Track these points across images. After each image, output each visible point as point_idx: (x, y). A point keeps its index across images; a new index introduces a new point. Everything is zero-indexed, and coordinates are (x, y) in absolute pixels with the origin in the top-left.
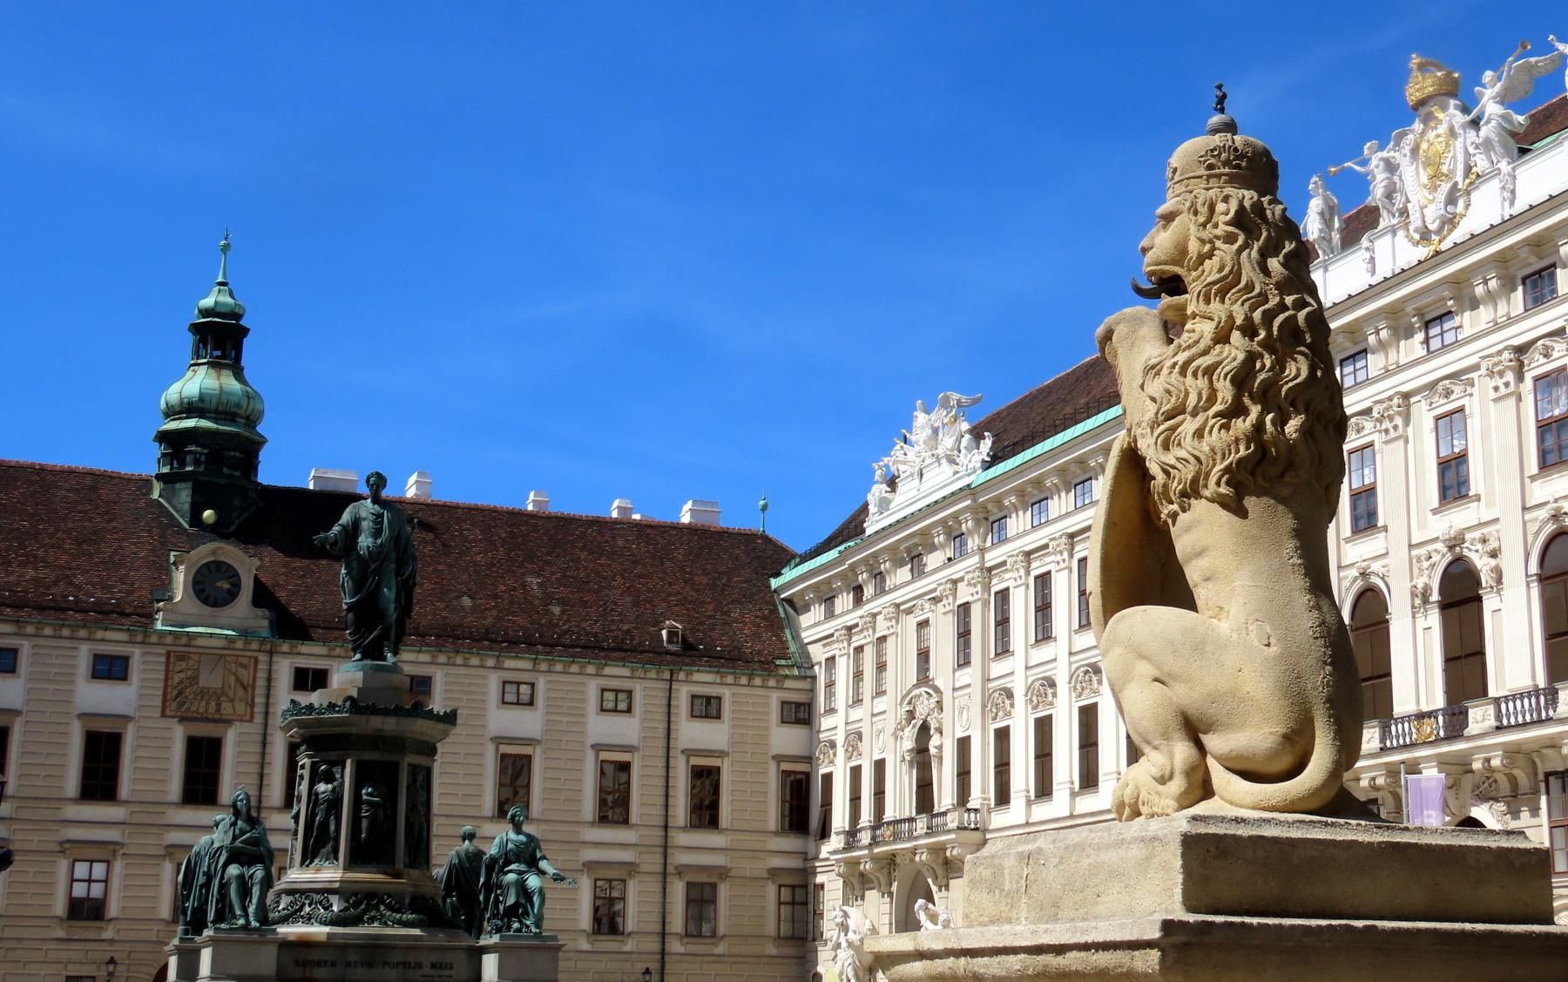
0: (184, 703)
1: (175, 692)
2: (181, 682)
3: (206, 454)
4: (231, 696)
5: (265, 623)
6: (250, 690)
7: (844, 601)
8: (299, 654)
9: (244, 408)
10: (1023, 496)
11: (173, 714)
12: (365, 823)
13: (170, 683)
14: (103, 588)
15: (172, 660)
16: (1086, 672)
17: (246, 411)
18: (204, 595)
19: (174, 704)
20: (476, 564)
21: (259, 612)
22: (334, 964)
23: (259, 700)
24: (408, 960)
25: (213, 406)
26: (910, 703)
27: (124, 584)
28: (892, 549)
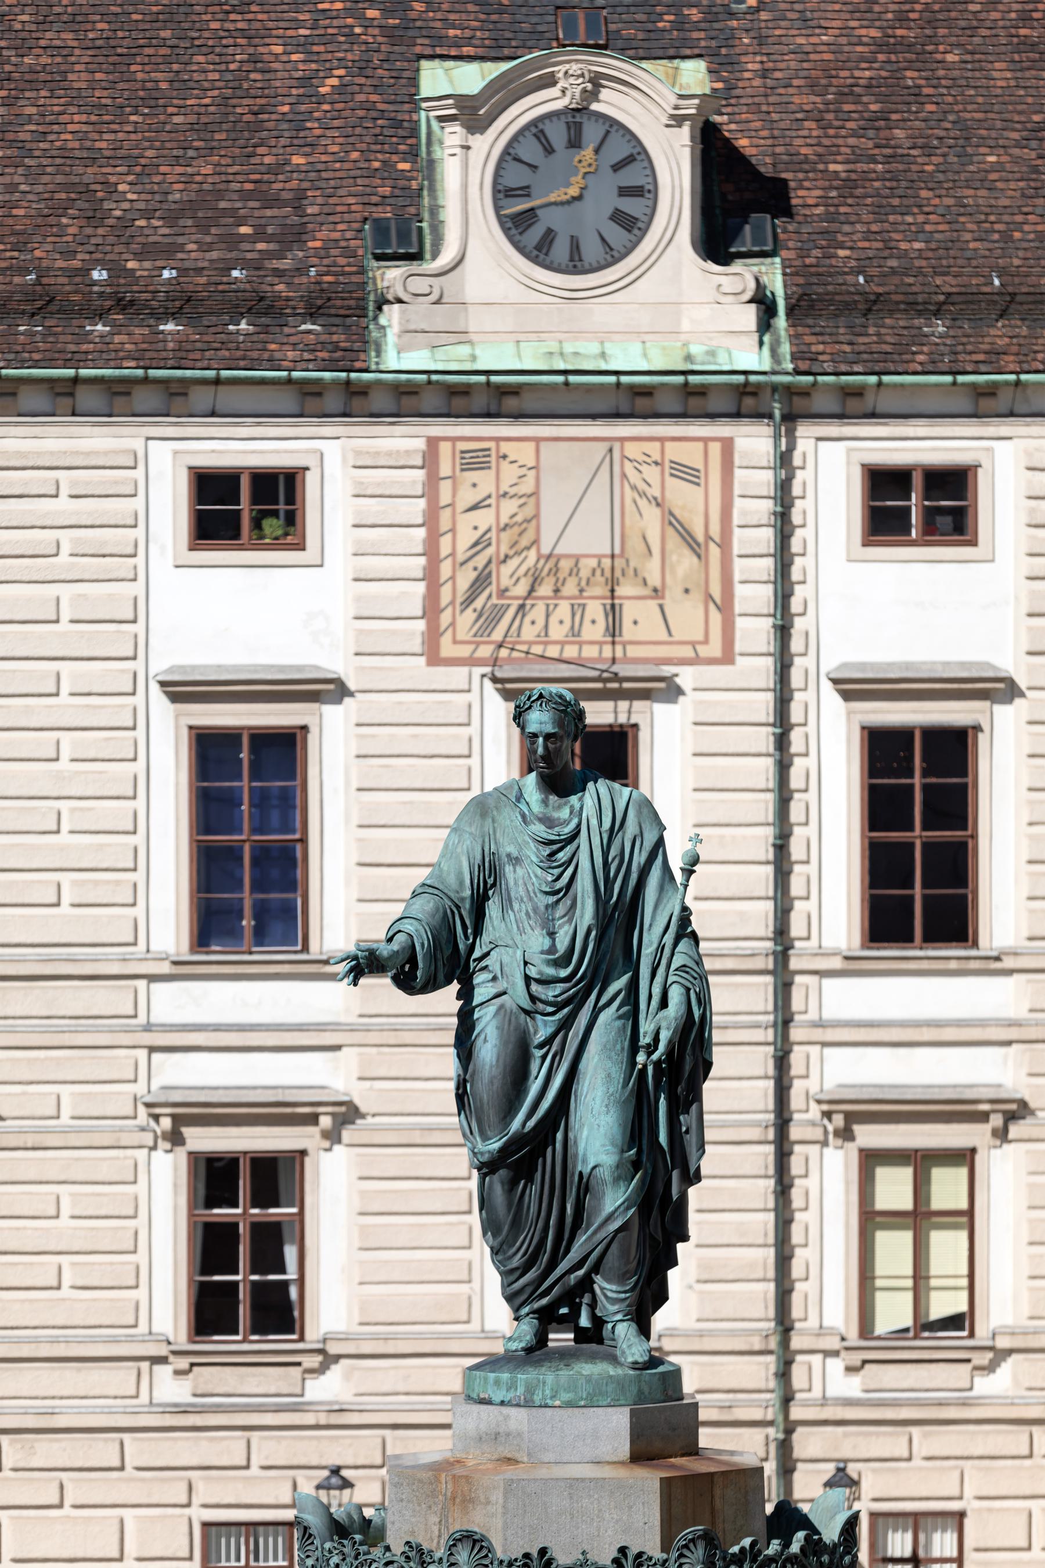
0: (498, 613)
1: (465, 579)
4: (654, 580)
5: (750, 316)
6: (714, 551)
11: (464, 651)
13: (445, 545)
14: (203, 227)
15: (445, 468)
18: (535, 234)
19: (470, 615)
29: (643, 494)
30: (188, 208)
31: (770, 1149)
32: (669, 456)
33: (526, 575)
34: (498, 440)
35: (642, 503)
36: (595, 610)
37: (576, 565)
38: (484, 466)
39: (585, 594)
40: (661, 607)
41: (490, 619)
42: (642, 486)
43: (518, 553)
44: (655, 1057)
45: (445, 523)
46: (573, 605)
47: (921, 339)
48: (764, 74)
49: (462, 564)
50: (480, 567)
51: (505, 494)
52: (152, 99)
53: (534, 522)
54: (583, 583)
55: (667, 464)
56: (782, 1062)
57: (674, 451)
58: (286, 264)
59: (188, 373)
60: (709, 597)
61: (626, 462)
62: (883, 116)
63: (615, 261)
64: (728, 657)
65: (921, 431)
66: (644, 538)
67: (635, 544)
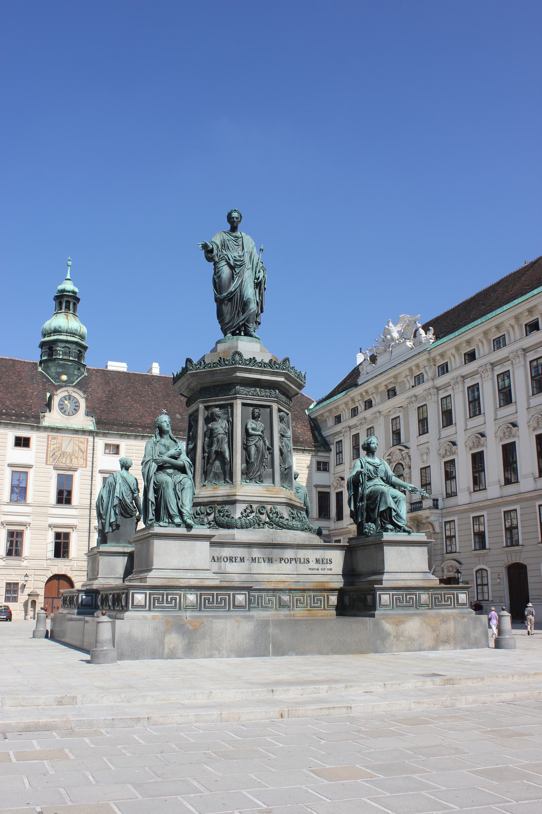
1: (51, 454)
6: (85, 453)
7: (346, 414)
9: (79, 331)
10: (459, 351)
11: (51, 463)
12: (253, 450)
13: (49, 449)
14: (18, 407)
15: (50, 439)
16: (508, 427)
17: (79, 334)
18: (63, 410)
19: (52, 458)
20: (181, 401)
21: (90, 418)
22: (242, 560)
23: (89, 459)
24: (299, 557)
26: (389, 455)
27: (28, 405)
28: (376, 387)
29: (76, 445)
30: (17, 405)
31: (88, 533)
36: (69, 459)
41: (54, 459)
44: (259, 281)
45: (49, 446)
47: (113, 428)
48: (91, 398)
52: (11, 393)
56: (90, 521)
58: (29, 412)
59: (16, 423)
60: (84, 459)
62: (107, 404)
63: (74, 415)
64: (86, 467)
65: (113, 440)
67: (74, 451)
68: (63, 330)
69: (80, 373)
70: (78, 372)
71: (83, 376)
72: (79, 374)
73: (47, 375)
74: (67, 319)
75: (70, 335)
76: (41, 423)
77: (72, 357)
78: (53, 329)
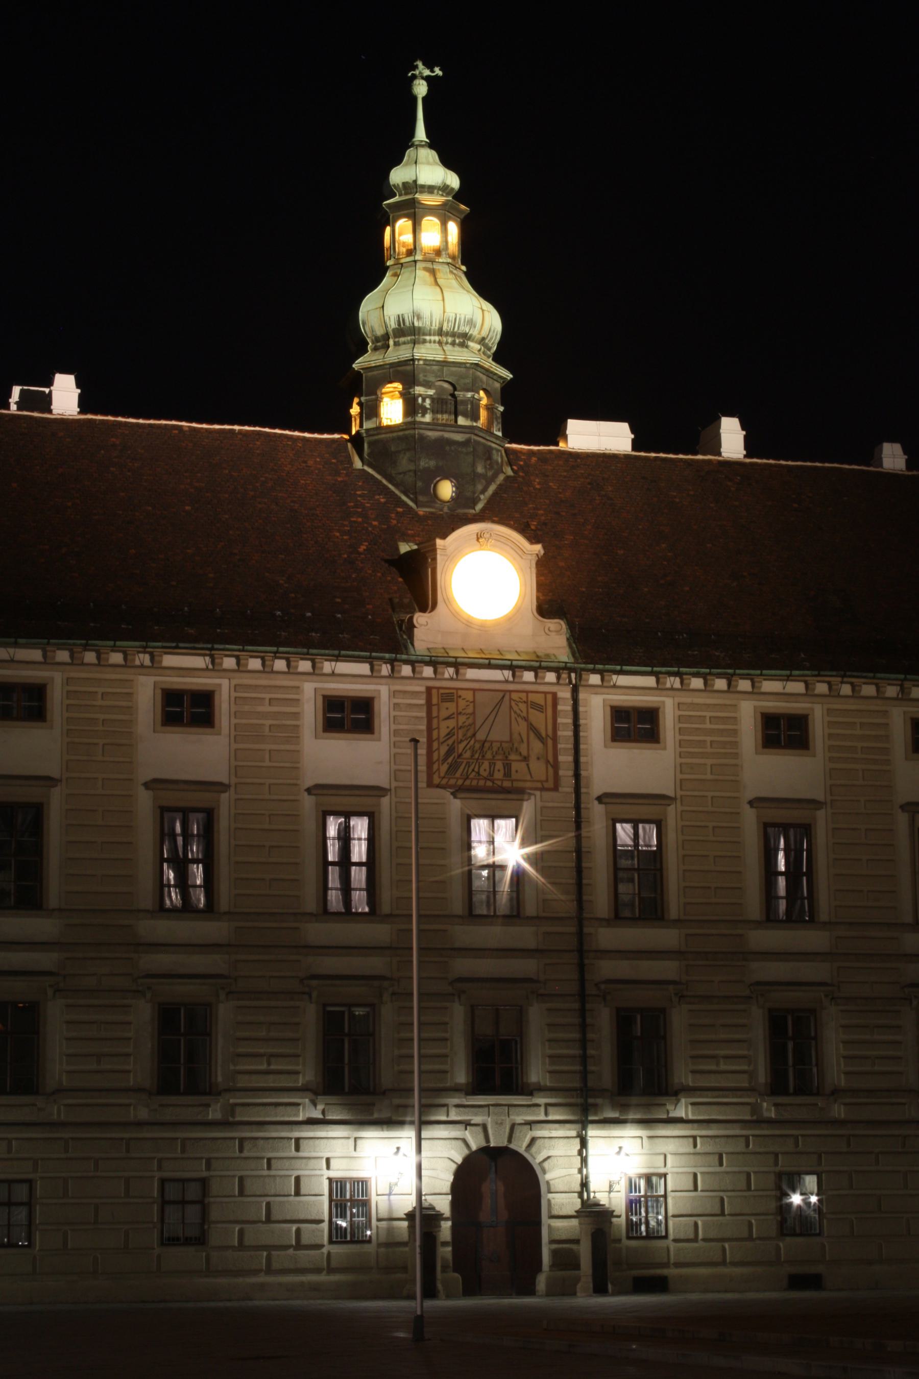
1: (444, 749)
2: (450, 734)
3: (430, 397)
4: (524, 753)
6: (550, 742)
8: (615, 686)
13: (435, 734)
15: (435, 701)
17: (479, 333)
19: (444, 768)
23: (566, 758)
25: (435, 327)
29: (519, 715)
32: (530, 699)
33: (470, 749)
34: (457, 689)
35: (519, 719)
36: (499, 765)
37: (491, 745)
38: (452, 701)
39: (496, 758)
40: (528, 765)
41: (453, 768)
42: (518, 712)
43: (466, 739)
45: (435, 725)
46: (490, 763)
49: (442, 743)
50: (450, 746)
51: (460, 713)
53: (473, 726)
54: (494, 753)
55: (529, 702)
57: (532, 697)
60: (548, 762)
61: (512, 702)
66: (520, 734)
67: (516, 736)
68: (428, 323)
69: (491, 467)
70: (485, 467)
71: (501, 477)
72: (490, 473)
73: (385, 482)
74: (437, 284)
75: (450, 340)
76: (404, 649)
77: (465, 415)
78: (393, 324)
